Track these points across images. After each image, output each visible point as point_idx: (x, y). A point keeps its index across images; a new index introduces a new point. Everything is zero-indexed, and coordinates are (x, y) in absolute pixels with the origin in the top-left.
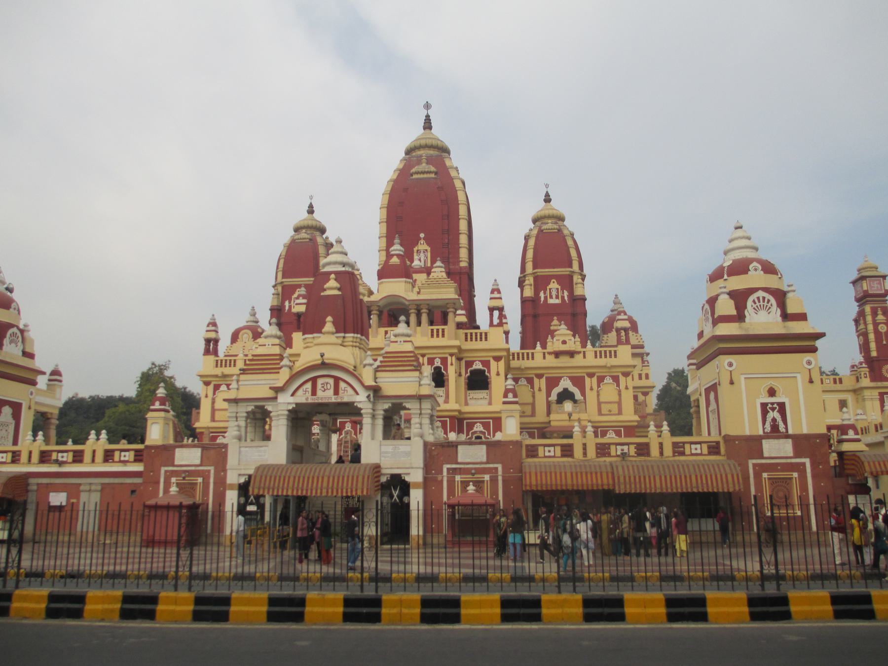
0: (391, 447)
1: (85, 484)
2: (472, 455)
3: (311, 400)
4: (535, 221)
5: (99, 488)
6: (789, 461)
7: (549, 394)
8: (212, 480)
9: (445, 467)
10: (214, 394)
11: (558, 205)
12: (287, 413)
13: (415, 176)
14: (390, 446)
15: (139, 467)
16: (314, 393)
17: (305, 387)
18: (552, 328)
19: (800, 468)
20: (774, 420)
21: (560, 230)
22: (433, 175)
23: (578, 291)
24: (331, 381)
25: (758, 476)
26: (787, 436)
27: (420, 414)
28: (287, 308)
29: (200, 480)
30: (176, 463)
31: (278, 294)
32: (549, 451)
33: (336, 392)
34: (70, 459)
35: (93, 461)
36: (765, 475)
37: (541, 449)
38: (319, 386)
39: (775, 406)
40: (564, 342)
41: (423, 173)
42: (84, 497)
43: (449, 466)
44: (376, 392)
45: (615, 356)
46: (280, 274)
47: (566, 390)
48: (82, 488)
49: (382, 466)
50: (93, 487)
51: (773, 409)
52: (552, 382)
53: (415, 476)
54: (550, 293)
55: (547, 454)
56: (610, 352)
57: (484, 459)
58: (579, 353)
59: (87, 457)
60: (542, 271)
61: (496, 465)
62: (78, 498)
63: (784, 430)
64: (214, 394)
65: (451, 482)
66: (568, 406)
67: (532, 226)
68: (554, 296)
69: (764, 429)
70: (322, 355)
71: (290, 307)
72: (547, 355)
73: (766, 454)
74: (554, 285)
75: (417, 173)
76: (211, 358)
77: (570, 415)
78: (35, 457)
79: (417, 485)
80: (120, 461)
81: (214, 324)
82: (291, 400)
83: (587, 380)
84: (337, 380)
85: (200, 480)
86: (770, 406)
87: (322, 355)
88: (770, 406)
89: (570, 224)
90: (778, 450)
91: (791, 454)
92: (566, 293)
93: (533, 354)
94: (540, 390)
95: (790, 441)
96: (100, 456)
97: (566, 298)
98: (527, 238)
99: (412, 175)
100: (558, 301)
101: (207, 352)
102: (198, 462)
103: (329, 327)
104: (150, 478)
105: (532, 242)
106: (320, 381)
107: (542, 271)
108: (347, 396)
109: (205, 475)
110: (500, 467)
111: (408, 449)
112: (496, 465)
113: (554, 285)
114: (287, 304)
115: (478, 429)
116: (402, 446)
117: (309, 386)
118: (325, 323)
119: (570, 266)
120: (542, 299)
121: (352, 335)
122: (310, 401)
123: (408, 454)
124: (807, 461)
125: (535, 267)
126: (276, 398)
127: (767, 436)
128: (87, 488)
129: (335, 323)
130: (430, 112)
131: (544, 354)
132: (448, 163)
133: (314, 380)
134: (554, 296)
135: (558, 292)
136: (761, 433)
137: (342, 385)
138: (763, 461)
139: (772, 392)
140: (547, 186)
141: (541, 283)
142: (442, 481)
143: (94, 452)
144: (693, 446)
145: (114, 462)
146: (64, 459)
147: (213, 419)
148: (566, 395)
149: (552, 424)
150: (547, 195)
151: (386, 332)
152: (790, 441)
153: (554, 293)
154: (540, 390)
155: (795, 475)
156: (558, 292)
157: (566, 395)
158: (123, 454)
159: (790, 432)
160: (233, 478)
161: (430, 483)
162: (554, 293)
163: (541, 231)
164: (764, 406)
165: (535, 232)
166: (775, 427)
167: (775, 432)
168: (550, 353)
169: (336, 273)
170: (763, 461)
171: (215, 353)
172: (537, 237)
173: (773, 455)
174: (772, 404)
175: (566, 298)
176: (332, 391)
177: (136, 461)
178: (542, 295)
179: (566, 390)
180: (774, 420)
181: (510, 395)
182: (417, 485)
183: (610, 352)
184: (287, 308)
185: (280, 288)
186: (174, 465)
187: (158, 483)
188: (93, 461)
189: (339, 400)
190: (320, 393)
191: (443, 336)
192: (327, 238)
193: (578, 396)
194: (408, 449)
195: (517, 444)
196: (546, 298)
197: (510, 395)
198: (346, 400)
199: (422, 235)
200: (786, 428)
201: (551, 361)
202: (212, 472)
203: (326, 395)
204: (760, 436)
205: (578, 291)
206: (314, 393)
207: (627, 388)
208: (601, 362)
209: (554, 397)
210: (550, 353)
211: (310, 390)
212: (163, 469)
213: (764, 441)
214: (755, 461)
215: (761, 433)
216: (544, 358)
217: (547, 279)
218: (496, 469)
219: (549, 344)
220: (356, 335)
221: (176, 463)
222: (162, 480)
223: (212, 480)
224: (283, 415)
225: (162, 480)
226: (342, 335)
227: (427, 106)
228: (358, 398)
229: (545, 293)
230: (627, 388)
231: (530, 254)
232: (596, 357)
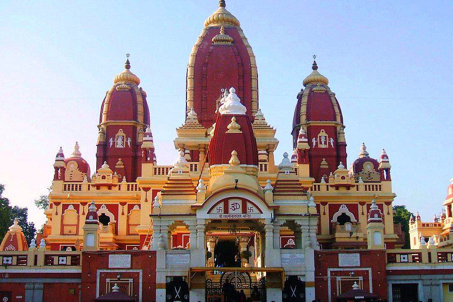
0: (289, 255)
1: (29, 283)
2: (349, 261)
3: (224, 217)
4: (305, 84)
5: (42, 286)
7: (331, 218)
8: (141, 281)
9: (329, 270)
10: (63, 212)
11: (322, 71)
12: (204, 227)
14: (287, 254)
15: (76, 270)
16: (226, 211)
17: (218, 206)
18: (321, 167)
21: (326, 92)
22: (230, 43)
23: (341, 140)
24: (240, 202)
28: (111, 144)
29: (131, 280)
31: (104, 133)
32: (404, 258)
33: (244, 211)
34: (15, 262)
35: (35, 264)
37: (398, 256)
38: (230, 206)
40: (343, 178)
42: (28, 294)
43: (332, 269)
44: (276, 210)
45: (380, 190)
46: (104, 116)
47: (344, 214)
48: (26, 286)
50: (37, 286)
52: (334, 208)
53: (310, 277)
54: (320, 140)
55: (402, 260)
56: (373, 186)
57: (359, 264)
58: (353, 186)
59: (31, 261)
60: (313, 123)
61: (367, 269)
62: (24, 295)
64: (63, 212)
65: (333, 282)
66: (348, 226)
67: (304, 88)
68: (323, 143)
70: (237, 181)
71: (114, 143)
72: (329, 187)
74: (323, 134)
75: (216, 40)
76: (61, 183)
77: (351, 233)
79: (310, 284)
80: (59, 265)
81: (62, 155)
82: (208, 216)
83: (360, 206)
84: (245, 201)
85: (131, 280)
87: (237, 181)
89: (333, 87)
92: (332, 141)
93: (319, 186)
94: (324, 214)
96: (41, 260)
97: (332, 144)
98: (300, 97)
100: (327, 146)
101: (56, 178)
102: (129, 266)
103: (233, 159)
104: (87, 278)
105: (305, 100)
106: (231, 202)
107: (313, 123)
108: (253, 215)
109: (135, 277)
110: (370, 270)
111: (302, 256)
112: (367, 269)
113: (323, 134)
114: (111, 140)
115: (291, 244)
116: (297, 254)
117: (222, 205)
119: (335, 120)
120: (314, 144)
121: (252, 166)
122: (223, 218)
123: (302, 260)
125: (308, 119)
128: (32, 286)
129: (239, 156)
131: (328, 187)
132: (241, 36)
133: (226, 201)
134: (323, 143)
135: (326, 139)
137: (249, 205)
140: (315, 57)
141: (311, 133)
142: (327, 281)
143: (36, 256)
145: (52, 264)
146: (10, 262)
147: (62, 233)
148: (344, 219)
149: (337, 240)
150: (315, 64)
153: (323, 140)
154: (324, 214)
156: (326, 139)
157: (344, 219)
158: (61, 258)
160: (161, 278)
161: (320, 284)
162: (323, 140)
163: (311, 91)
165: (307, 92)
168: (331, 186)
169: (236, 116)
171: (63, 178)
172: (309, 96)
175: (332, 144)
176: (240, 211)
177: (72, 264)
178: (314, 140)
179: (344, 214)
181: (376, 215)
182: (310, 284)
183: (373, 186)
184: (111, 144)
185: (105, 129)
186: (108, 268)
187: (95, 282)
188: (35, 264)
189: (247, 218)
190: (231, 211)
191: (266, 170)
192: (141, 88)
193: (353, 219)
194: (302, 256)
195: (382, 252)
196: (317, 143)
197: (376, 215)
198: (253, 217)
201: (332, 191)
202: (141, 274)
203: (236, 213)
205: (341, 140)
206: (226, 211)
207: (388, 213)
208: (371, 193)
209: (335, 219)
210: (331, 186)
211: (223, 209)
212: (99, 271)
216: (328, 190)
217: (318, 129)
218: (368, 271)
219: (330, 179)
222: (98, 280)
223: (141, 281)
224: (200, 229)
225: (98, 280)
226: (246, 165)
228: (262, 216)
229: (316, 140)
230: (388, 213)
231: (303, 109)
232: (366, 190)
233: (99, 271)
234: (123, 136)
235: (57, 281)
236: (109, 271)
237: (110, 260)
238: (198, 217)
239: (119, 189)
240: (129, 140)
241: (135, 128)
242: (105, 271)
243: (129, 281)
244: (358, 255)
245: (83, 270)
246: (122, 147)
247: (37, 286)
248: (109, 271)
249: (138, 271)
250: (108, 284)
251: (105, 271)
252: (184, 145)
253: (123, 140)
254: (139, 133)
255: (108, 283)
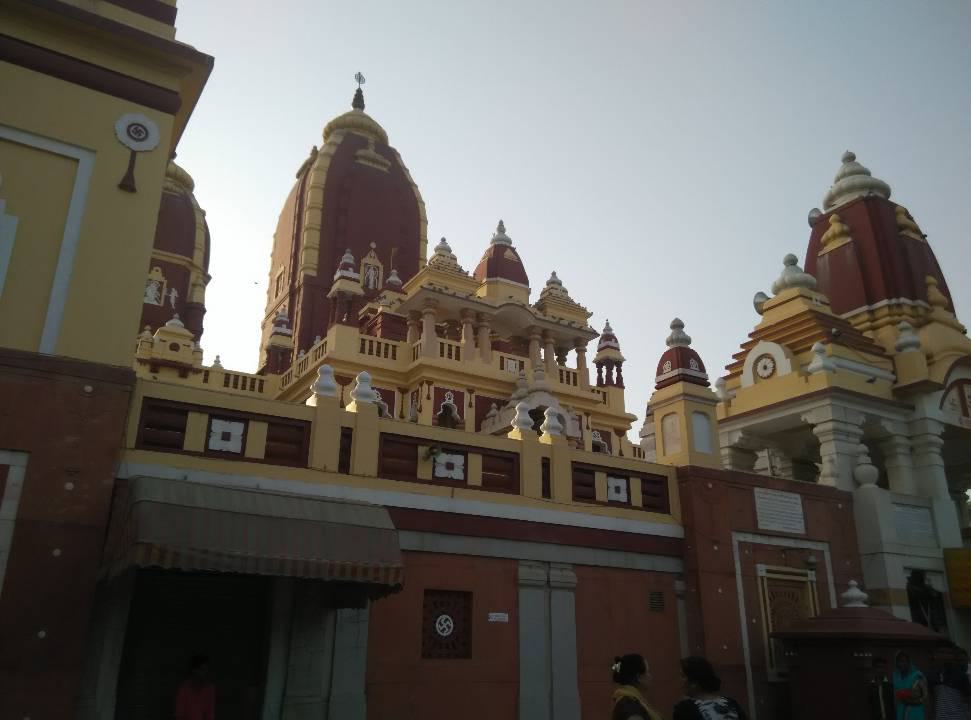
13: (362, 162)
22: (385, 169)
30: (762, 525)
41: (374, 161)
62: (513, 609)
75: (365, 158)
78: (366, 454)
99: (356, 158)
102: (799, 528)
118: (926, 286)
126: (913, 408)
128: (540, 574)
130: (362, 87)
151: (502, 358)
187: (733, 574)
199: (373, 245)
211: (957, 402)
221: (762, 525)
222: (738, 566)
225: (738, 566)
227: (360, 78)
233: (738, 538)
234: (161, 283)
235: (616, 559)
236: (759, 540)
237: (759, 502)
239: (206, 380)
240: (174, 294)
241: (187, 274)
242: (750, 538)
243: (806, 575)
245: (688, 524)
246: (155, 303)
247: (556, 575)
248: (759, 540)
249: (819, 547)
250: (762, 580)
251: (750, 538)
252: (437, 301)
253: (160, 290)
254: (194, 285)
255: (762, 578)
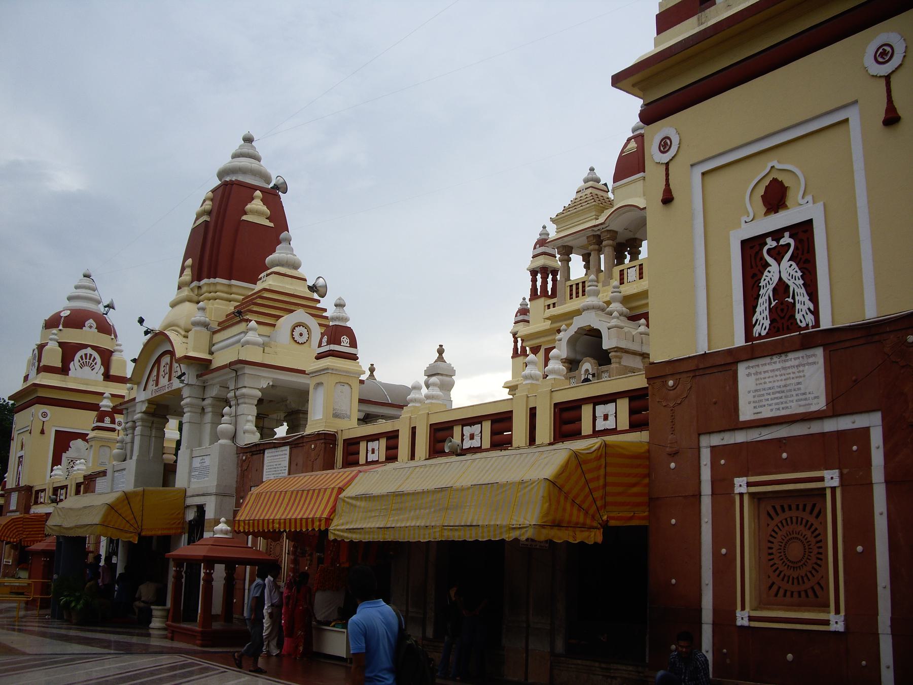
6: (816, 428)
19: (847, 451)
20: (782, 289)
25: (722, 487)
26: (808, 341)
27: (235, 397)
36: (740, 485)
39: (786, 239)
49: (188, 494)
51: (778, 254)
63: (810, 318)
69: (749, 326)
73: (746, 413)
86: (771, 243)
88: (771, 243)
90: (782, 389)
91: (820, 404)
95: (818, 354)
124: (872, 422)
127: (754, 350)
136: (739, 340)
138: (740, 437)
139: (775, 197)
144: (601, 410)
151: (622, 272)
152: (819, 352)
155: (831, 478)
159: (826, 323)
164: (752, 249)
166: (783, 314)
167: (784, 332)
170: (740, 437)
173: (767, 413)
174: (777, 235)
180: (782, 289)
200: (815, 313)
204: (730, 352)
213: (742, 370)
214: (716, 440)
215: (739, 340)
220: (212, 280)
226: (195, 283)
238: (137, 400)
244: (288, 448)
